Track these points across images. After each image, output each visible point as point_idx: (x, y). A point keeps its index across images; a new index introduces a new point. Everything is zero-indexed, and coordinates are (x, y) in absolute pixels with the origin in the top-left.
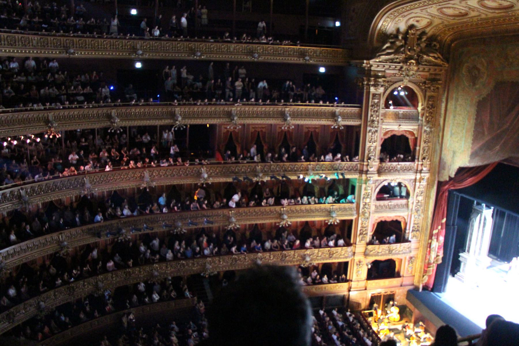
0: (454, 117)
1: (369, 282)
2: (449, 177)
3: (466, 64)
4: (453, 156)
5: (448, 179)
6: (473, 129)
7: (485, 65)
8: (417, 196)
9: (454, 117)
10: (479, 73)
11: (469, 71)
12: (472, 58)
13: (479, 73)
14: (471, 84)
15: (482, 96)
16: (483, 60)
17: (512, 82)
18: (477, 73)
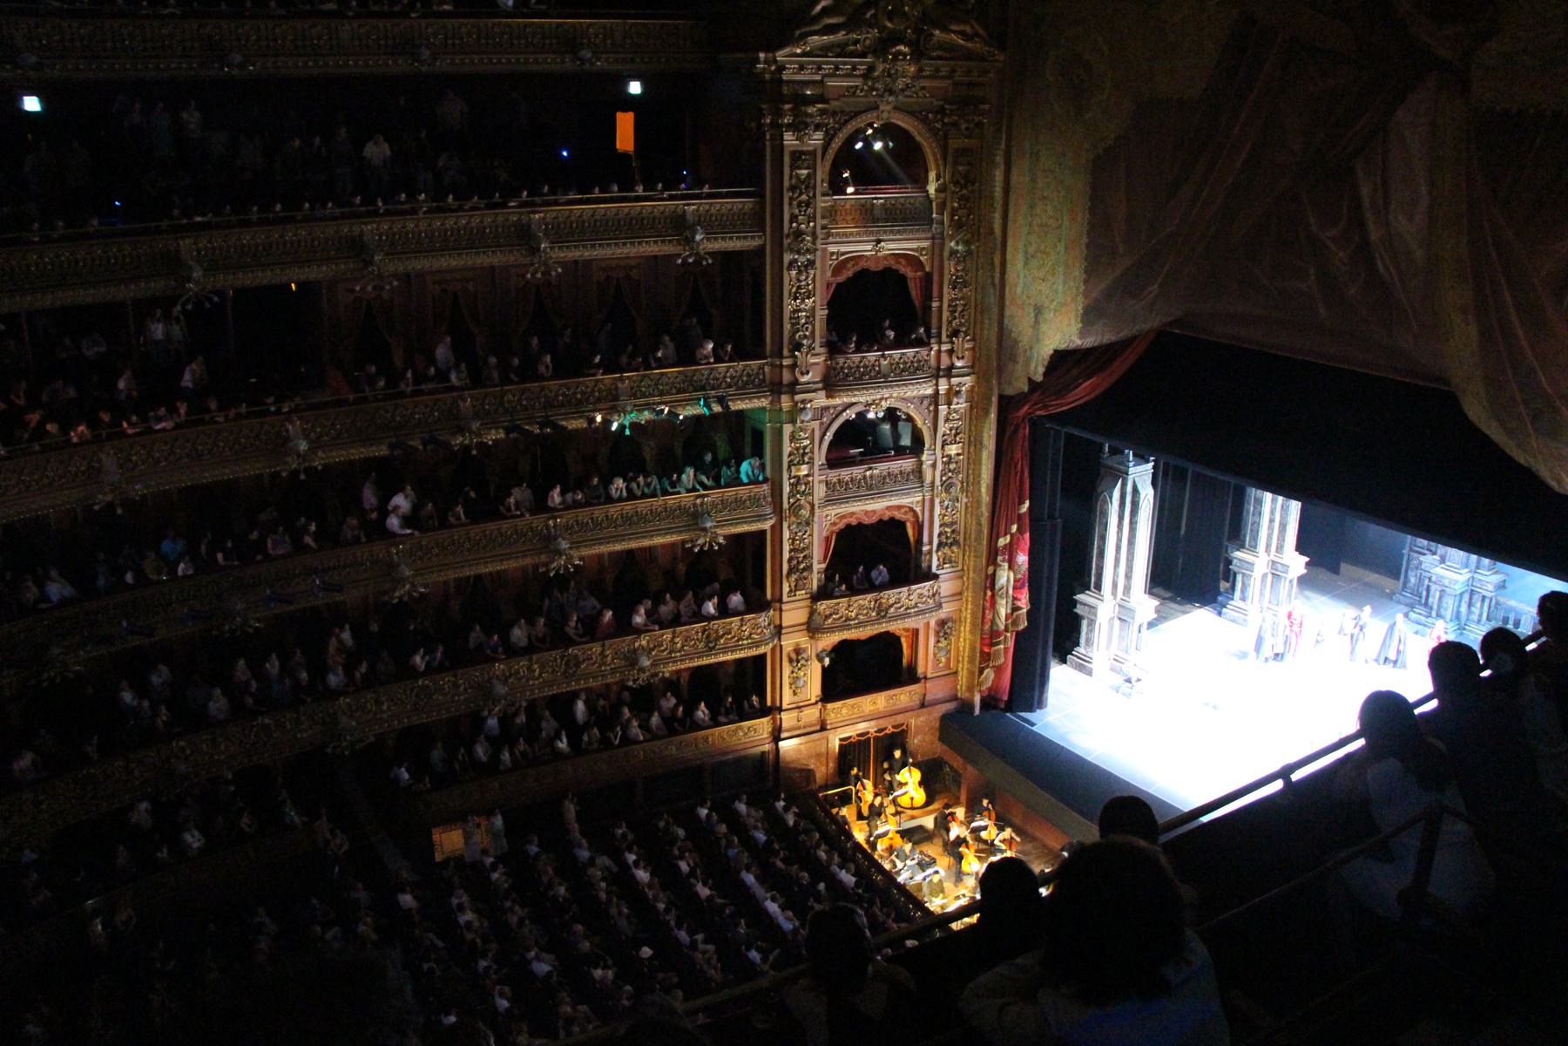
0: (1032, 207)
1: (829, 706)
2: (1030, 380)
4: (1037, 322)
5: (1026, 389)
6: (1085, 240)
8: (944, 444)
9: (1032, 207)
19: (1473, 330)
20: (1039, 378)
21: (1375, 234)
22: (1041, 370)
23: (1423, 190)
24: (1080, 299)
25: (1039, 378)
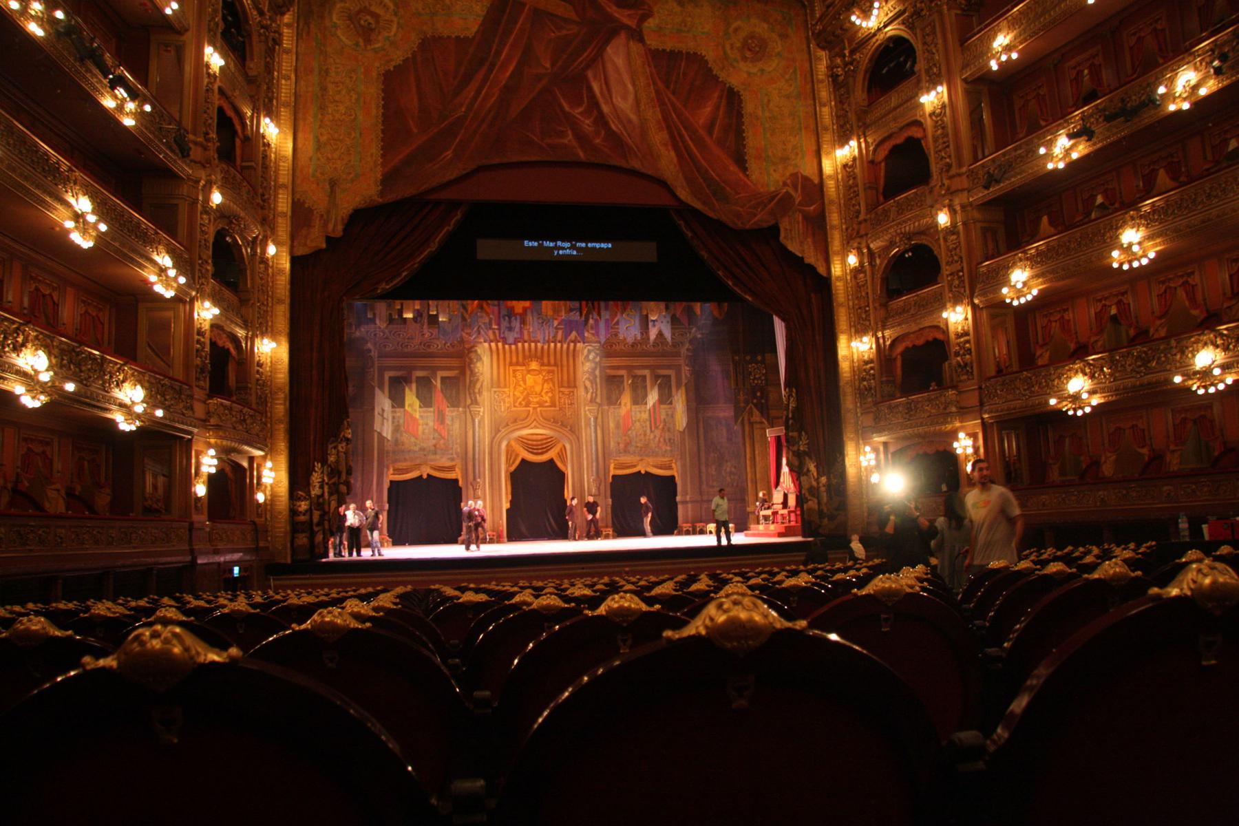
0: (322, 108)
2: (329, 240)
3: (338, 6)
4: (333, 191)
5: (324, 246)
7: (392, 6)
9: (322, 108)
10: (377, 22)
11: (351, 18)
14: (361, 40)
15: (393, 64)
17: (458, 37)
18: (371, 20)
19: (673, 154)
20: (339, 232)
21: (605, 109)
22: (340, 228)
23: (630, 87)
24: (379, 168)
25: (339, 232)
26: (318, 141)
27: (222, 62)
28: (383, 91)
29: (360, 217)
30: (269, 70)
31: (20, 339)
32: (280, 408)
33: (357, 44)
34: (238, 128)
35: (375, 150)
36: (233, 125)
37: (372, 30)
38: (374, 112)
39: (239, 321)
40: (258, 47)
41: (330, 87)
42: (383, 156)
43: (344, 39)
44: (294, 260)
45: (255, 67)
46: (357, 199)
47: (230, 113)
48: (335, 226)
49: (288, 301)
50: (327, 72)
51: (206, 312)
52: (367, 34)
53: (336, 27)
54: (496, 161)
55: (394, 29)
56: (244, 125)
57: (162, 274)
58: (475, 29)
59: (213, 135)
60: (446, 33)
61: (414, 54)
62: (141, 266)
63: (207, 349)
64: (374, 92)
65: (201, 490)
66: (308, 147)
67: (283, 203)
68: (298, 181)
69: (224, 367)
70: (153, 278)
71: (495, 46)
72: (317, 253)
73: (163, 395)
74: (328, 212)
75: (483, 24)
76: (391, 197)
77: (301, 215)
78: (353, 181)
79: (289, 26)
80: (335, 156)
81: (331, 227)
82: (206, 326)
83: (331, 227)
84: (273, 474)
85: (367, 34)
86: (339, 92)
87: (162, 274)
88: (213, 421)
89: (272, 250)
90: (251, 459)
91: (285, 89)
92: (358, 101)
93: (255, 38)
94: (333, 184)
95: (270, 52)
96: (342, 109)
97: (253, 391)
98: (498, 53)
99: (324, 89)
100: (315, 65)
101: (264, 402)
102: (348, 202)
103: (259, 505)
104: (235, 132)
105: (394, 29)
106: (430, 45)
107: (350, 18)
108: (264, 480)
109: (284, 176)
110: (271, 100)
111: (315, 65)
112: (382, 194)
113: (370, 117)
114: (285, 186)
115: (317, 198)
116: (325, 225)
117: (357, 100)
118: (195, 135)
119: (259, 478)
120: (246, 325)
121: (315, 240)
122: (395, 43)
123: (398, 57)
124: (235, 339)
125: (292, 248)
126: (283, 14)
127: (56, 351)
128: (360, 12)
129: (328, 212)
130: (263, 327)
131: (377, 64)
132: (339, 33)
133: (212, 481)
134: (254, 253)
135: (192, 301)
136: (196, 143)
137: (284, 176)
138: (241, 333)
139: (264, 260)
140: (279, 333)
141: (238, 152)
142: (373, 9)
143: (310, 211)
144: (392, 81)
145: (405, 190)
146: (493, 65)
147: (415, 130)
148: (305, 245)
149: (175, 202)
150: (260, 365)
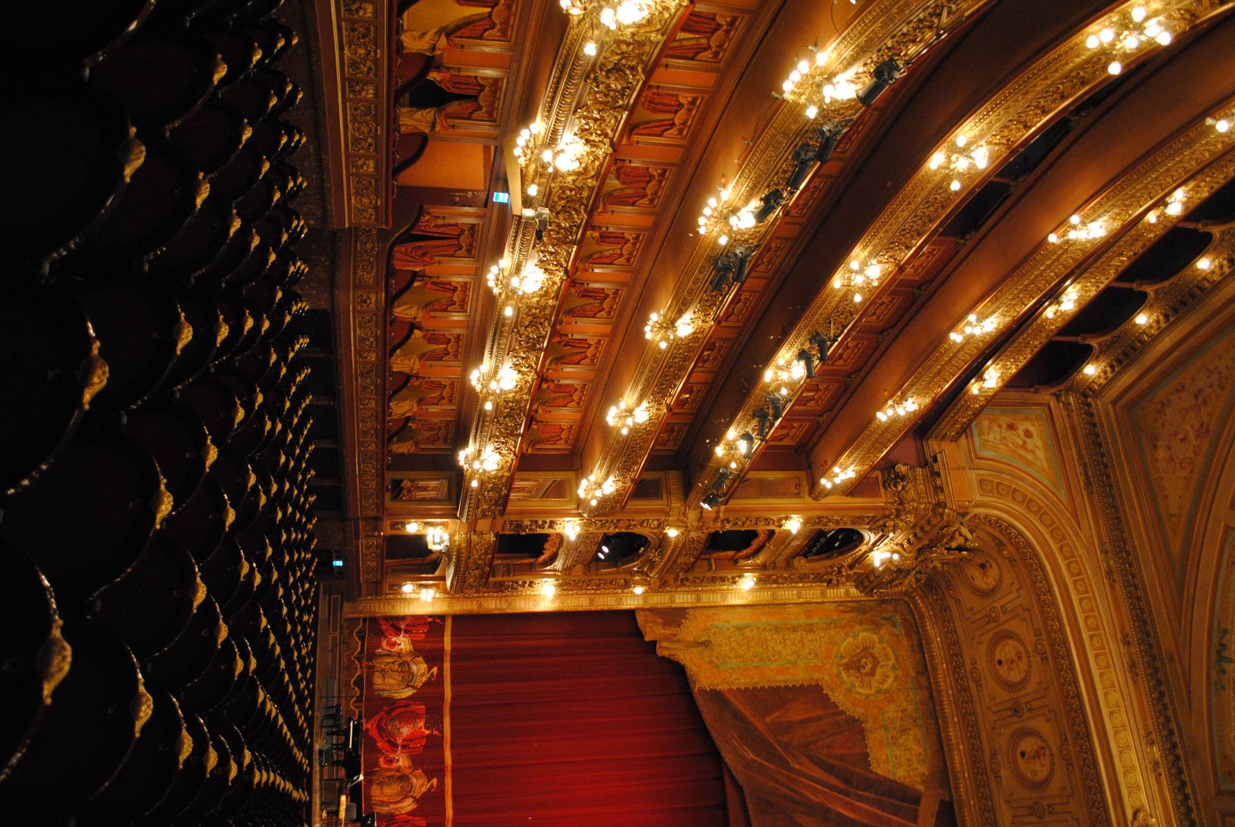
2: (654, 643)
3: (875, 637)
4: (700, 644)
5: (647, 639)
7: (885, 687)
10: (867, 675)
11: (866, 650)
12: (889, 651)
13: (867, 675)
15: (830, 693)
16: (890, 680)
17: (867, 755)
20: (661, 652)
22: (666, 653)
24: (726, 687)
25: (661, 652)
26: (745, 627)
27: (794, 531)
28: (802, 686)
29: (678, 670)
30: (803, 578)
31: (524, 369)
32: (492, 604)
33: (842, 657)
34: (744, 552)
35: (744, 681)
36: (745, 548)
37: (858, 670)
38: (780, 678)
39: (569, 562)
40: (820, 565)
41: (798, 635)
42: (738, 689)
43: (845, 644)
44: (631, 613)
45: (801, 564)
46: (695, 668)
47: (755, 544)
48: (667, 648)
49: (593, 608)
50: (811, 631)
51: (571, 529)
52: (854, 665)
53: (855, 637)
54: (750, 806)
55: (863, 691)
56: (747, 557)
57: (599, 484)
58: (879, 772)
59: (728, 527)
60: (871, 742)
61: (843, 712)
62: (601, 467)
63: (539, 531)
64: (799, 676)
65: (412, 528)
66: (737, 619)
67: (682, 599)
68: (705, 612)
69: (526, 548)
70: (592, 478)
71: (866, 794)
72: (639, 634)
73: (492, 489)
74: (679, 641)
75: (886, 779)
76: (700, 700)
77: (674, 616)
78: (711, 662)
79: (847, 593)
80: (734, 645)
81: (665, 644)
82: (558, 529)
83: (665, 644)
84: (429, 600)
85: (854, 665)
86: (793, 644)
87: (599, 484)
88: (474, 538)
89: (639, 590)
90: (443, 578)
91: (788, 594)
92: (791, 660)
93: (827, 563)
94: (706, 644)
95: (818, 578)
96: (779, 648)
97: (506, 578)
98: (860, 798)
99: (794, 629)
100: (815, 620)
101: (500, 588)
102: (691, 660)
103: (400, 586)
104: (739, 550)
105: (863, 691)
106: (855, 727)
107: (865, 649)
108: (424, 591)
109: (707, 599)
110: (775, 582)
111: (815, 620)
112: (702, 691)
113: (775, 675)
114: (699, 600)
115: (691, 630)
116: (666, 639)
117: (789, 661)
118: (726, 510)
119: (426, 586)
120: (567, 570)
121: (652, 631)
122: (849, 694)
123: (837, 697)
124: (553, 558)
125: (643, 610)
126: (857, 587)
127: (518, 397)
128: (874, 658)
129: (679, 641)
130: (567, 584)
131: (826, 677)
132: (850, 640)
133: (419, 540)
134: (633, 574)
135: (580, 515)
136: (718, 512)
137: (707, 599)
138: (558, 564)
139: (627, 585)
140: (563, 602)
141: (723, 554)
142: (879, 670)
143: (679, 625)
144: (813, 693)
145: (708, 714)
146: (847, 794)
147: (768, 720)
148: (646, 622)
149: (665, 496)
150: (531, 584)
